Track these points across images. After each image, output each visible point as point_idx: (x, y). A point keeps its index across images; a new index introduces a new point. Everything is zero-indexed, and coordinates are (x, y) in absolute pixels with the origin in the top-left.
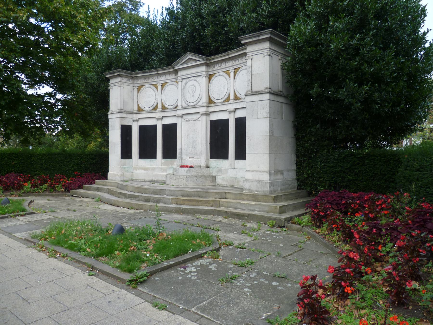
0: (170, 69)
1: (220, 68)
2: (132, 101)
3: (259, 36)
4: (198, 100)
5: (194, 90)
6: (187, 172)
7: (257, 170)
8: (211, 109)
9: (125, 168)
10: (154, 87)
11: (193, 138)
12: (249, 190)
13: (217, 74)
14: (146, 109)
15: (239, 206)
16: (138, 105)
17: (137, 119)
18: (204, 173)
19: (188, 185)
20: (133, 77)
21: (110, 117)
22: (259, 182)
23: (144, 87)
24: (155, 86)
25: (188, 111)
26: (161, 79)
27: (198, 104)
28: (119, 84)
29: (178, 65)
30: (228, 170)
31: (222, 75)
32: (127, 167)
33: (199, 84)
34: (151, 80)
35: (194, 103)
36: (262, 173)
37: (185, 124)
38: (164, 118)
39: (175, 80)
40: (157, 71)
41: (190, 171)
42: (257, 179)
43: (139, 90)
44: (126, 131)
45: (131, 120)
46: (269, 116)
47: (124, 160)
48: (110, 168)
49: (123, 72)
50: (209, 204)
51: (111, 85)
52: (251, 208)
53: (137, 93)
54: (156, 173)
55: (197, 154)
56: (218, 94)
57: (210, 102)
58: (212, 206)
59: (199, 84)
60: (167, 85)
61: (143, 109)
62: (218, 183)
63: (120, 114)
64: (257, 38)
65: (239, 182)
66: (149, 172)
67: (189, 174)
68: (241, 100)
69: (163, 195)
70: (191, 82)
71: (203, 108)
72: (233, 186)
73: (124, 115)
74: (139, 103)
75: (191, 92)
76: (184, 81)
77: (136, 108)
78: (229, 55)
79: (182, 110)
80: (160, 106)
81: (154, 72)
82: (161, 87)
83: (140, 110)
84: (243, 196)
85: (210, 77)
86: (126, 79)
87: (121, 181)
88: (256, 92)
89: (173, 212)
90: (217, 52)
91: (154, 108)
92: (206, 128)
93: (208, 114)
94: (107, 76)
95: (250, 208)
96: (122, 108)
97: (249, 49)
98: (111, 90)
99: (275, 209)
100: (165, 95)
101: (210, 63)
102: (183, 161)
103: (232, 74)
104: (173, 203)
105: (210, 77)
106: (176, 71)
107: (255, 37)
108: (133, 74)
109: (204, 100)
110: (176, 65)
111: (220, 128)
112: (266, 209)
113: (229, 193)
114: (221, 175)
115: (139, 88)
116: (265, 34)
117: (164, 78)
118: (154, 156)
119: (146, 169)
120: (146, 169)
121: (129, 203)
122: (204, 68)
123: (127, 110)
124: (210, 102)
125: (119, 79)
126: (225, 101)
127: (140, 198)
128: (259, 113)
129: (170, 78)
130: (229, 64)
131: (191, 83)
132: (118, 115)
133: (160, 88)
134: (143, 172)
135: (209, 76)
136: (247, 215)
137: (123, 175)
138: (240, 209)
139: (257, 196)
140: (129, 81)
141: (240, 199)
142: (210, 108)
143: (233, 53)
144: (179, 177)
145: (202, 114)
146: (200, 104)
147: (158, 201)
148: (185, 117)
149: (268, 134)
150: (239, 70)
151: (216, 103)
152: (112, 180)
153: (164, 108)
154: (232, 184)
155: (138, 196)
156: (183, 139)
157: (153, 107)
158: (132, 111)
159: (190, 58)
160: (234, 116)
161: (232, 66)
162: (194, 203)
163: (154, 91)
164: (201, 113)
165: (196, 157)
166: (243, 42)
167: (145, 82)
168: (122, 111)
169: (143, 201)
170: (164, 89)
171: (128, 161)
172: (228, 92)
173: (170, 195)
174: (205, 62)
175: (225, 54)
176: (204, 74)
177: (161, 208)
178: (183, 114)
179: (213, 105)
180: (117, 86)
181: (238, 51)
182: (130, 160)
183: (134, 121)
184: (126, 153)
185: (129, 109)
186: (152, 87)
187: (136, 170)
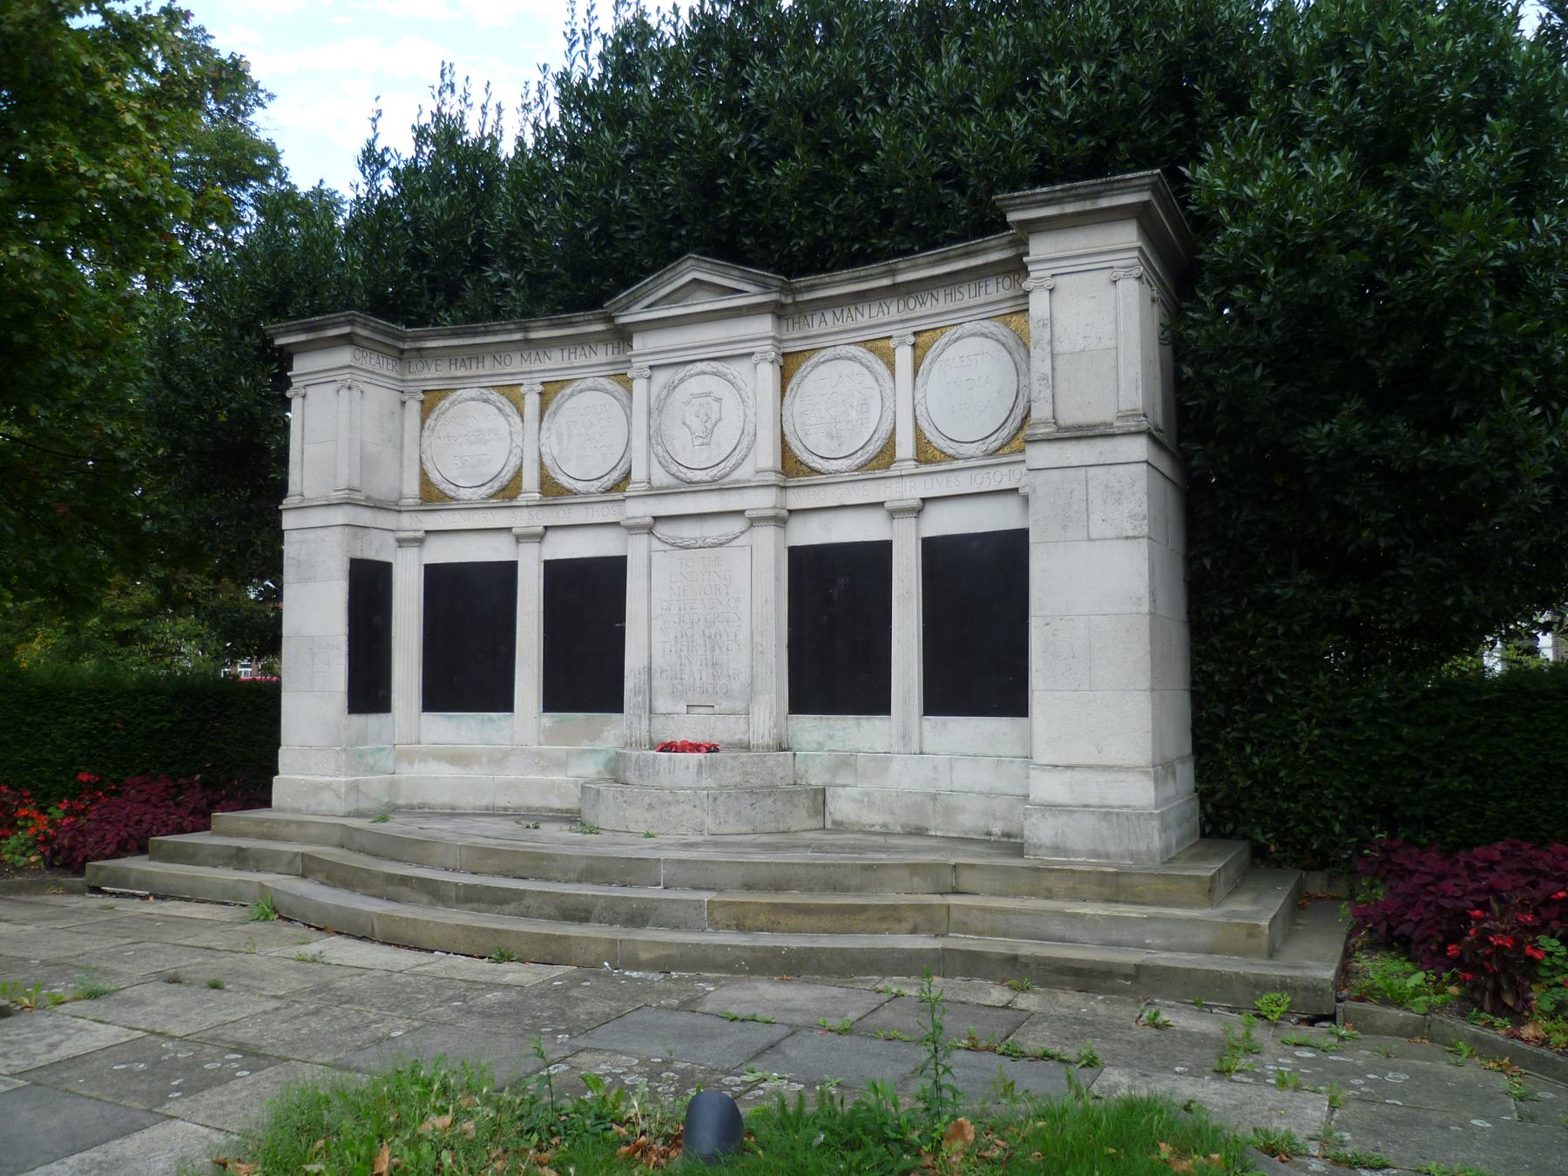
0: (589, 322)
1: (840, 326)
2: (385, 457)
3: (1097, 195)
4: (732, 461)
5: (714, 418)
6: (699, 772)
7: (1092, 762)
8: (798, 499)
9: (361, 755)
10: (504, 400)
11: (706, 623)
12: (1056, 850)
14: (462, 493)
15: (1056, 928)
16: (424, 475)
17: (420, 534)
18: (772, 774)
19: (714, 828)
20: (402, 351)
21: (288, 521)
22: (1107, 813)
23: (453, 396)
24: (511, 392)
25: (688, 504)
26: (537, 366)
27: (734, 476)
28: (345, 376)
30: (908, 761)
31: (853, 359)
32: (374, 751)
33: (738, 389)
34: (488, 367)
35: (714, 471)
36: (1121, 776)
37: (666, 562)
38: (550, 535)
39: (609, 370)
40: (526, 330)
41: (713, 766)
42: (1095, 801)
43: (426, 410)
44: (369, 587)
45: (390, 538)
46: (1145, 530)
47: (359, 720)
48: (285, 757)
49: (365, 326)
50: (899, 921)
51: (297, 383)
52: (1125, 936)
53: (418, 421)
54: (511, 775)
55: (728, 694)
56: (831, 436)
57: (791, 467)
58: (914, 931)
59: (738, 389)
60: (568, 391)
61: (450, 490)
62: (838, 817)
63: (348, 508)
64: (1087, 205)
65: (950, 811)
66: (475, 774)
67: (708, 782)
68: (957, 464)
69: (642, 885)
70: (698, 383)
71: (761, 491)
72: (919, 832)
73: (365, 517)
74: (429, 467)
75: (696, 424)
76: (661, 377)
77: (412, 487)
78: (893, 272)
79: (651, 501)
80: (530, 480)
81: (510, 332)
82: (537, 397)
83: (432, 496)
84: (1050, 881)
85: (788, 366)
86: (374, 356)
87: (348, 815)
88: (1080, 428)
89: (740, 971)
90: (817, 260)
91: (503, 489)
92: (777, 579)
93: (781, 520)
94: (279, 342)
95: (1115, 936)
96: (356, 484)
97: (1040, 247)
98: (296, 403)
99: (1250, 936)
100: (559, 436)
101: (795, 303)
102: (658, 723)
103: (904, 356)
104: (716, 925)
105: (788, 366)
106: (623, 336)
108: (403, 339)
109: (766, 456)
110: (627, 307)
111: (842, 582)
112: (1204, 937)
113: (973, 866)
114: (850, 781)
115: (430, 402)
116: (1124, 188)
117: (555, 363)
118: (501, 699)
119: (459, 759)
120: (459, 759)
121: (484, 930)
122: (764, 325)
123: (374, 496)
124: (791, 467)
125: (345, 356)
126: (860, 468)
127: (528, 901)
128: (1095, 517)
129: (582, 361)
130: (893, 310)
131: (694, 386)
132: (340, 516)
133: (531, 403)
134: (447, 772)
135: (781, 361)
136: (1131, 971)
137: (354, 787)
138: (1062, 940)
139: (1124, 880)
140: (386, 367)
141: (1032, 894)
142: (791, 494)
143: (915, 267)
144: (670, 798)
145: (754, 522)
146: (744, 473)
147: (638, 917)
148: (663, 530)
149: (1145, 608)
150: (944, 340)
151: (819, 472)
152: (298, 811)
153: (552, 490)
154: (914, 821)
155: (520, 895)
156: (656, 625)
157: (496, 485)
158: (394, 497)
159: (695, 280)
160: (917, 531)
161: (902, 321)
162: (826, 921)
163: (506, 416)
164: (755, 514)
165: (724, 705)
166: (1012, 217)
167: (460, 373)
168: (357, 496)
169: (550, 917)
170: (552, 407)
171: (373, 721)
172: (886, 428)
173: (681, 886)
174: (773, 297)
176: (767, 347)
177: (674, 951)
178: (656, 518)
179: (805, 480)
180: (333, 387)
181: (945, 260)
182: (383, 717)
183: (401, 542)
184: (368, 689)
185: (381, 488)
186: (494, 396)
187: (411, 763)
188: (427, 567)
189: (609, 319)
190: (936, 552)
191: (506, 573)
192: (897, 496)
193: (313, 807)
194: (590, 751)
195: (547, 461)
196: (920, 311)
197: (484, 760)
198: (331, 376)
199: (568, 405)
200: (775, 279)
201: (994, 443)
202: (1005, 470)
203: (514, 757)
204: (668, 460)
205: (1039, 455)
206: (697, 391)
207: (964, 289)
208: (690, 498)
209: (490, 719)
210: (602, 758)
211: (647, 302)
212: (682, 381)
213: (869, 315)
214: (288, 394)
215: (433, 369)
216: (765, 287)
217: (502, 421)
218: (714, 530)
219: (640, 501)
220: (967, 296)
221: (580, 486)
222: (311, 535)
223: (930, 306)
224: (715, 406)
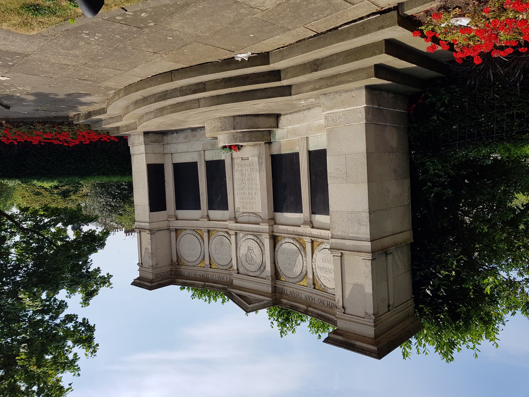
29: (265, 302)
65: (186, 138)
76: (264, 275)
122: (236, 282)
127: (153, 100)
154: (194, 133)
193: (337, 96)
201: (184, 232)
211: (262, 303)
213: (216, 277)
218: (245, 219)
221: (292, 241)
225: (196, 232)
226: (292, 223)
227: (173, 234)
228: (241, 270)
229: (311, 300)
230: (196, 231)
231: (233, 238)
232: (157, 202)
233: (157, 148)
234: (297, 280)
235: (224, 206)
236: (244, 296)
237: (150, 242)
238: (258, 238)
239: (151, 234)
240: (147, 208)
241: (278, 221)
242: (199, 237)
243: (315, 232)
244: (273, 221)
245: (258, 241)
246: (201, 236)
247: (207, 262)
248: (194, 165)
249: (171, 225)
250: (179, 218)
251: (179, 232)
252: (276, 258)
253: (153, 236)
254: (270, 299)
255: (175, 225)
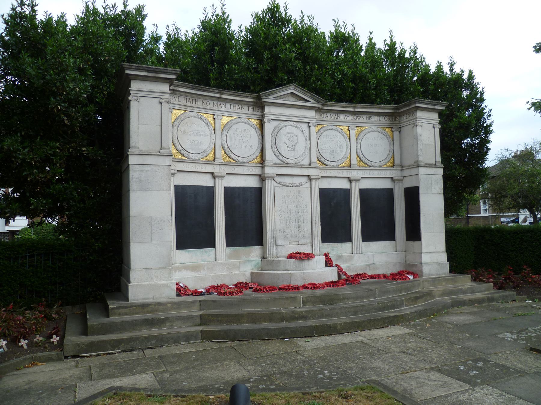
0: (247, 97)
1: (332, 119)
3: (435, 105)
7: (434, 251)
12: (429, 275)
13: (329, 127)
14: (191, 156)
21: (132, 160)
27: (302, 163)
29: (270, 97)
34: (200, 104)
35: (296, 161)
37: (280, 191)
40: (221, 94)
42: (435, 261)
48: (134, 276)
66: (203, 273)
68: (370, 168)
70: (288, 130)
71: (314, 169)
76: (275, 123)
79: (275, 168)
81: (214, 92)
97: (419, 114)
100: (231, 138)
102: (280, 249)
106: (259, 105)
107: (432, 105)
116: (441, 105)
118: (210, 243)
119: (195, 268)
120: (195, 268)
122: (312, 114)
125: (165, 88)
128: (433, 188)
129: (238, 111)
130: (350, 118)
143: (362, 108)
148: (278, 179)
159: (292, 93)
167: (189, 104)
175: (352, 105)
188: (175, 186)
189: (259, 98)
190: (363, 193)
191: (210, 191)
192: (353, 176)
194: (249, 261)
195: (226, 148)
196: (358, 120)
197: (206, 268)
198: (158, 95)
199: (234, 127)
200: (323, 101)
201: (383, 163)
202: (388, 172)
203: (221, 265)
204: (277, 153)
205: (422, 170)
206: (289, 131)
207: (372, 117)
208: (290, 169)
209: (206, 252)
210: (254, 263)
211: (275, 96)
212: (283, 127)
213: (342, 117)
214: (130, 98)
215: (177, 99)
216: (318, 102)
217: (207, 128)
219: (271, 168)
220: (373, 119)
221: (240, 159)
222: (149, 168)
223: (361, 120)
224: (295, 138)
225: (367, 164)
226: (239, 176)
227: (397, 161)
228: (304, 126)
229: (219, 104)
230: (368, 166)
231: (314, 159)
232: (412, 196)
233: (411, 259)
234: (234, 121)
235: (324, 194)
236: (300, 100)
237: (420, 152)
238: (281, 160)
239: (417, 162)
240: (421, 191)
241: (257, 178)
242: (363, 159)
243: (209, 168)
244: (262, 178)
245: (281, 157)
246: (361, 160)
247: (353, 133)
248: (367, 237)
249: (399, 172)
250: (389, 180)
251: (390, 164)
252: (261, 141)
253: (416, 159)
254: (265, 100)
255: (394, 171)
